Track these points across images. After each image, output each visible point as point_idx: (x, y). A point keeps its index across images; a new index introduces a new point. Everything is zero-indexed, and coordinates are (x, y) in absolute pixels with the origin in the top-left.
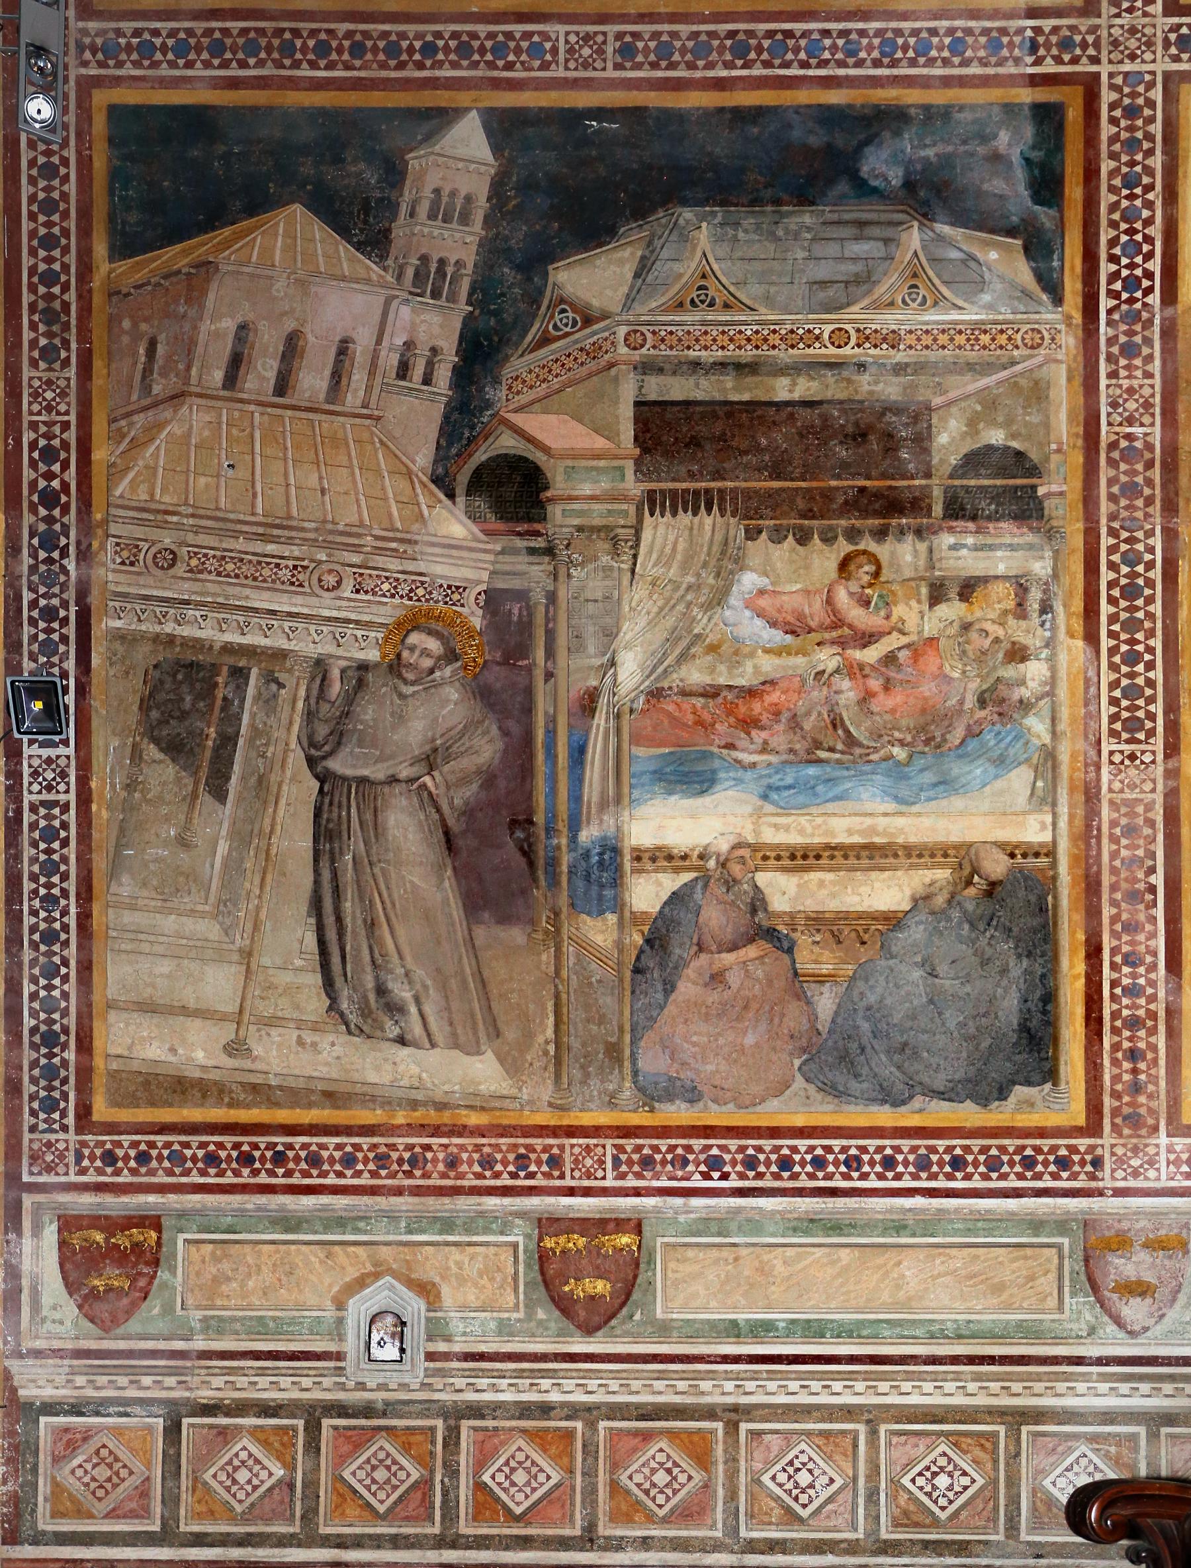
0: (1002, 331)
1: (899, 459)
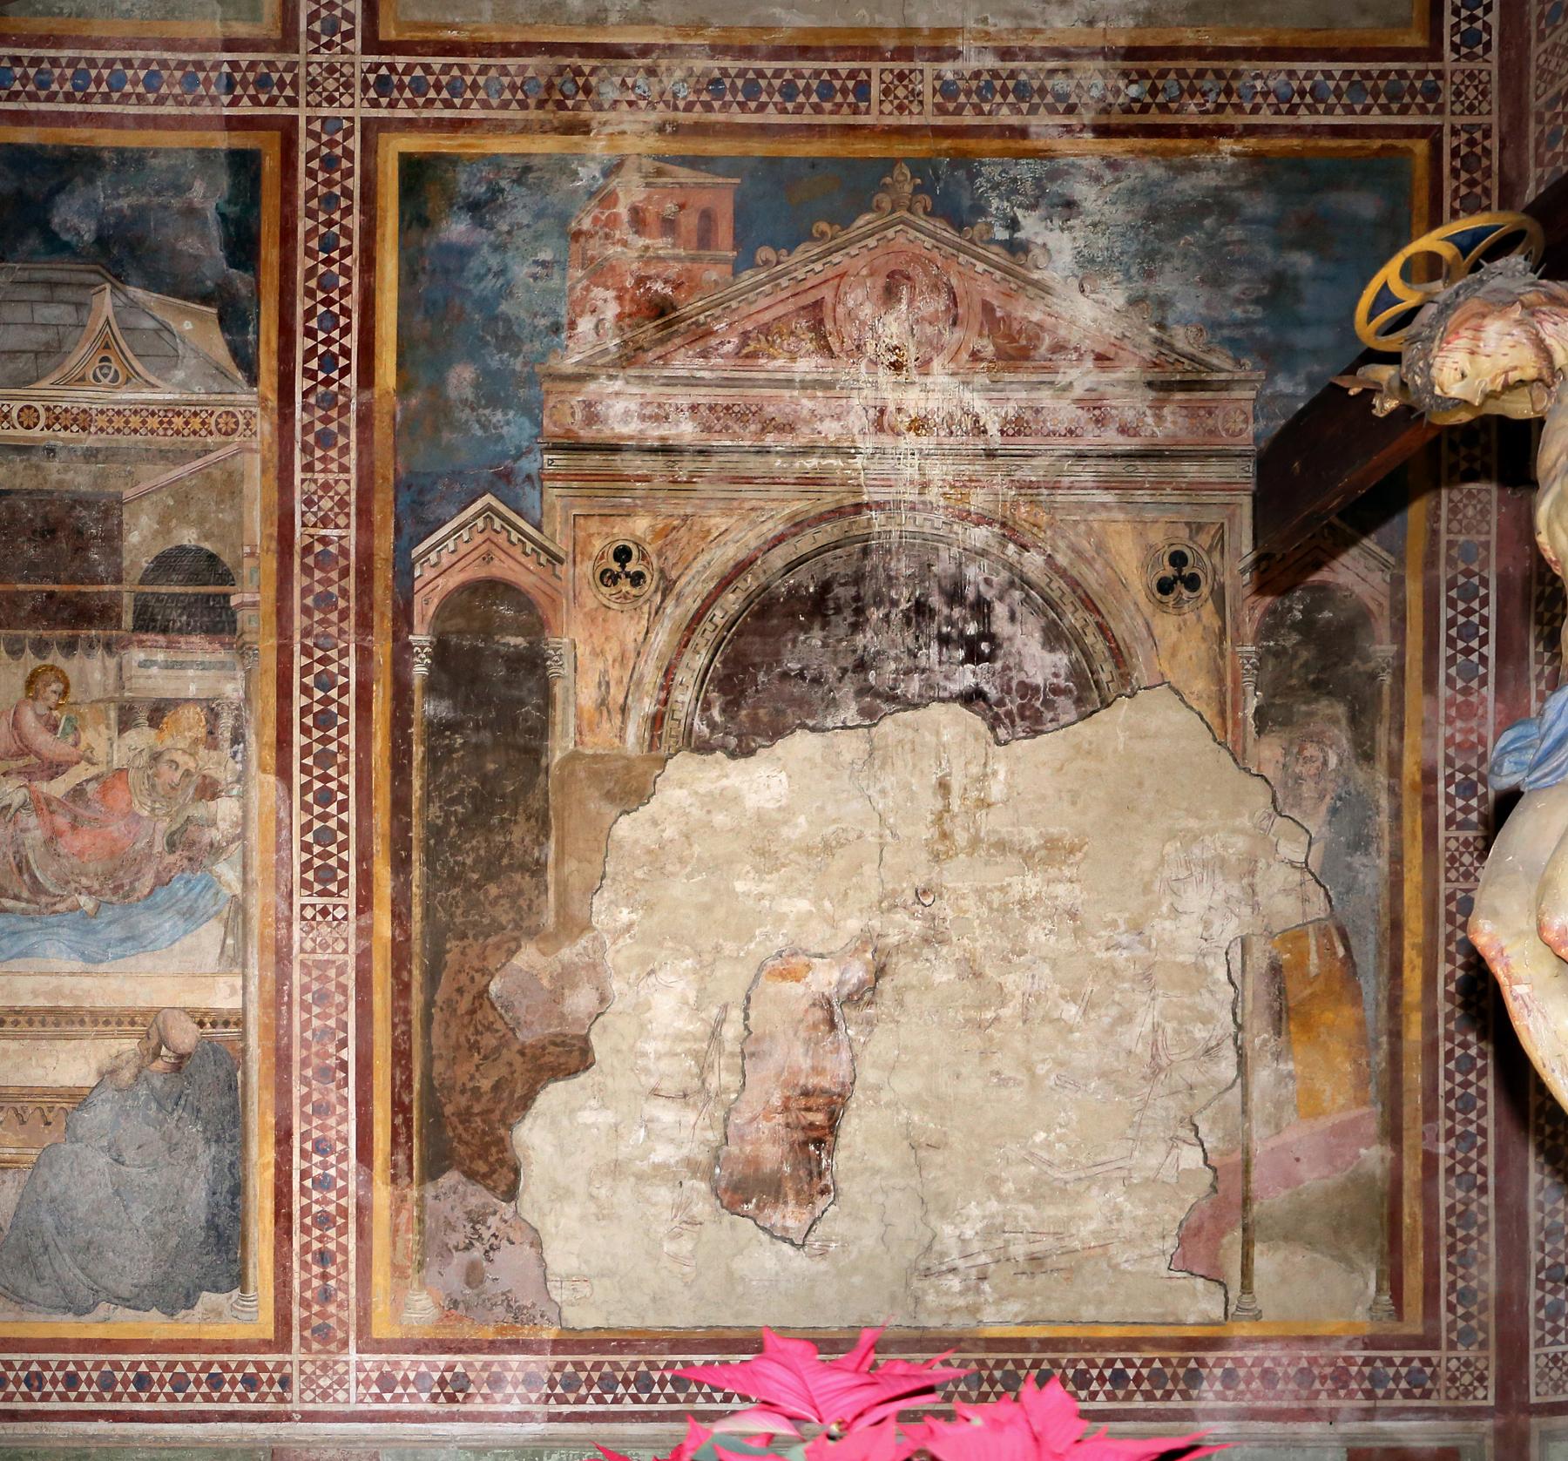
0: (195, 414)
1: (87, 559)
